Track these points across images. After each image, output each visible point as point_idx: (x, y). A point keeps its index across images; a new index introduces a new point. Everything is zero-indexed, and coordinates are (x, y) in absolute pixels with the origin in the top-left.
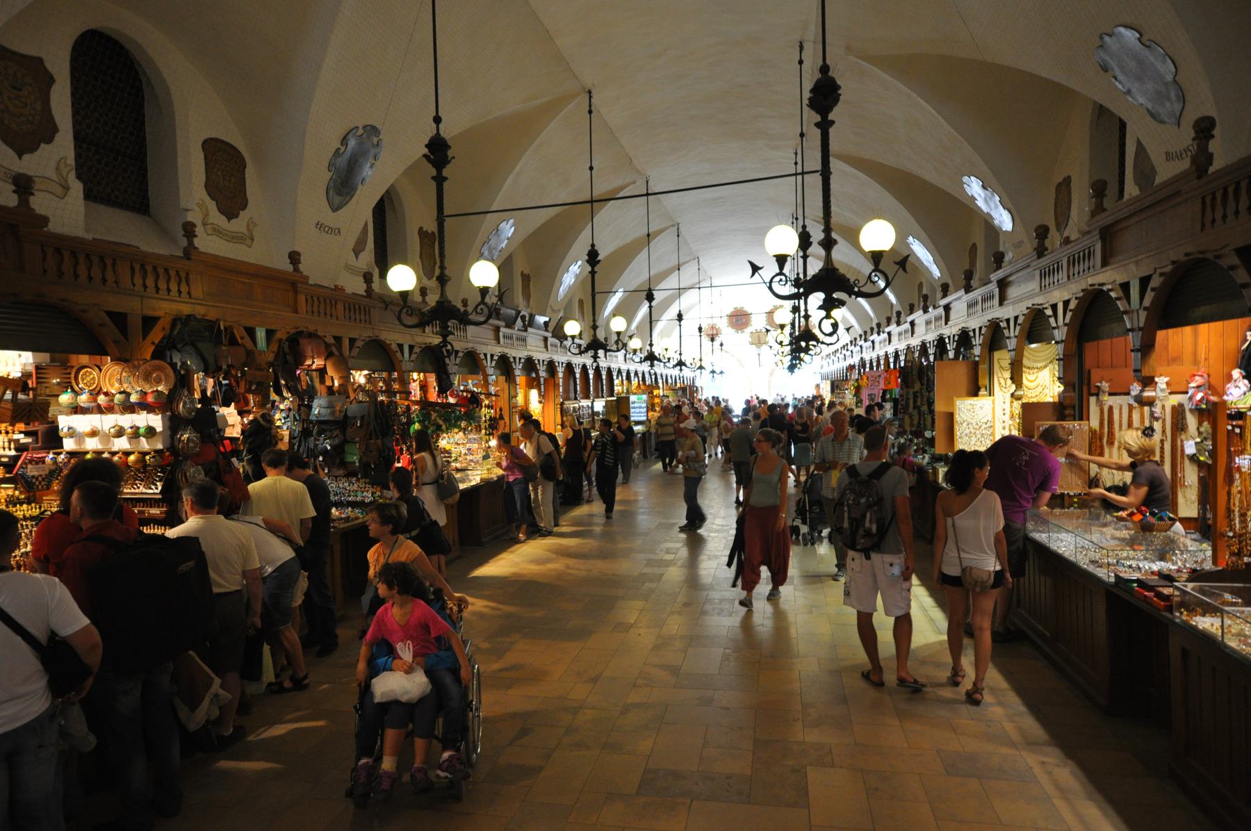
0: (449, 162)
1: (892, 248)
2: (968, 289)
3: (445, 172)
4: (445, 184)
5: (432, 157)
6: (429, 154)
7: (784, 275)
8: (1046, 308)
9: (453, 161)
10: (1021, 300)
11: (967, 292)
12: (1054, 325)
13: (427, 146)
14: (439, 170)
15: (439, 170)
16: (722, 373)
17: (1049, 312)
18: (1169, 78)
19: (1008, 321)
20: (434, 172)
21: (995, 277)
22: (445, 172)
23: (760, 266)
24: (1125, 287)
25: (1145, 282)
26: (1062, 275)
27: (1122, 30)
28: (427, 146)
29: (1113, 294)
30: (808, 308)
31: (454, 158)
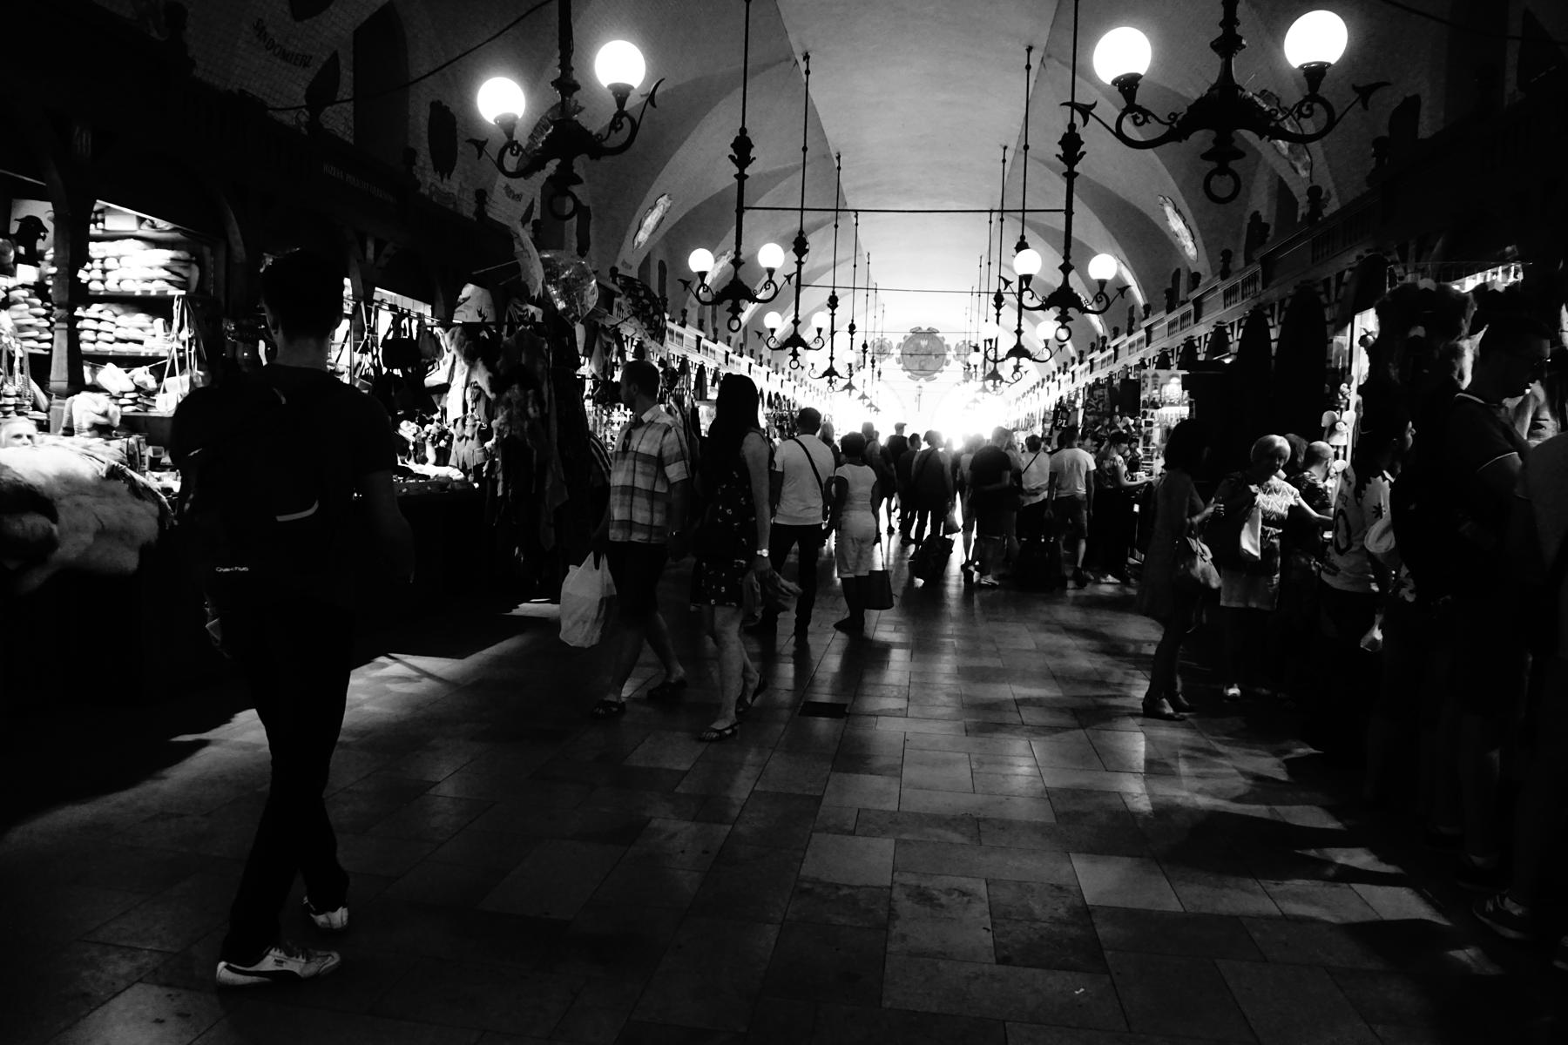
0: (751, 162)
4: (745, 181)
5: (736, 157)
6: (733, 154)
7: (1030, 290)
9: (754, 162)
13: (732, 146)
14: (742, 169)
15: (742, 169)
17: (1228, 330)
20: (736, 171)
22: (747, 171)
23: (1011, 280)
31: (754, 158)
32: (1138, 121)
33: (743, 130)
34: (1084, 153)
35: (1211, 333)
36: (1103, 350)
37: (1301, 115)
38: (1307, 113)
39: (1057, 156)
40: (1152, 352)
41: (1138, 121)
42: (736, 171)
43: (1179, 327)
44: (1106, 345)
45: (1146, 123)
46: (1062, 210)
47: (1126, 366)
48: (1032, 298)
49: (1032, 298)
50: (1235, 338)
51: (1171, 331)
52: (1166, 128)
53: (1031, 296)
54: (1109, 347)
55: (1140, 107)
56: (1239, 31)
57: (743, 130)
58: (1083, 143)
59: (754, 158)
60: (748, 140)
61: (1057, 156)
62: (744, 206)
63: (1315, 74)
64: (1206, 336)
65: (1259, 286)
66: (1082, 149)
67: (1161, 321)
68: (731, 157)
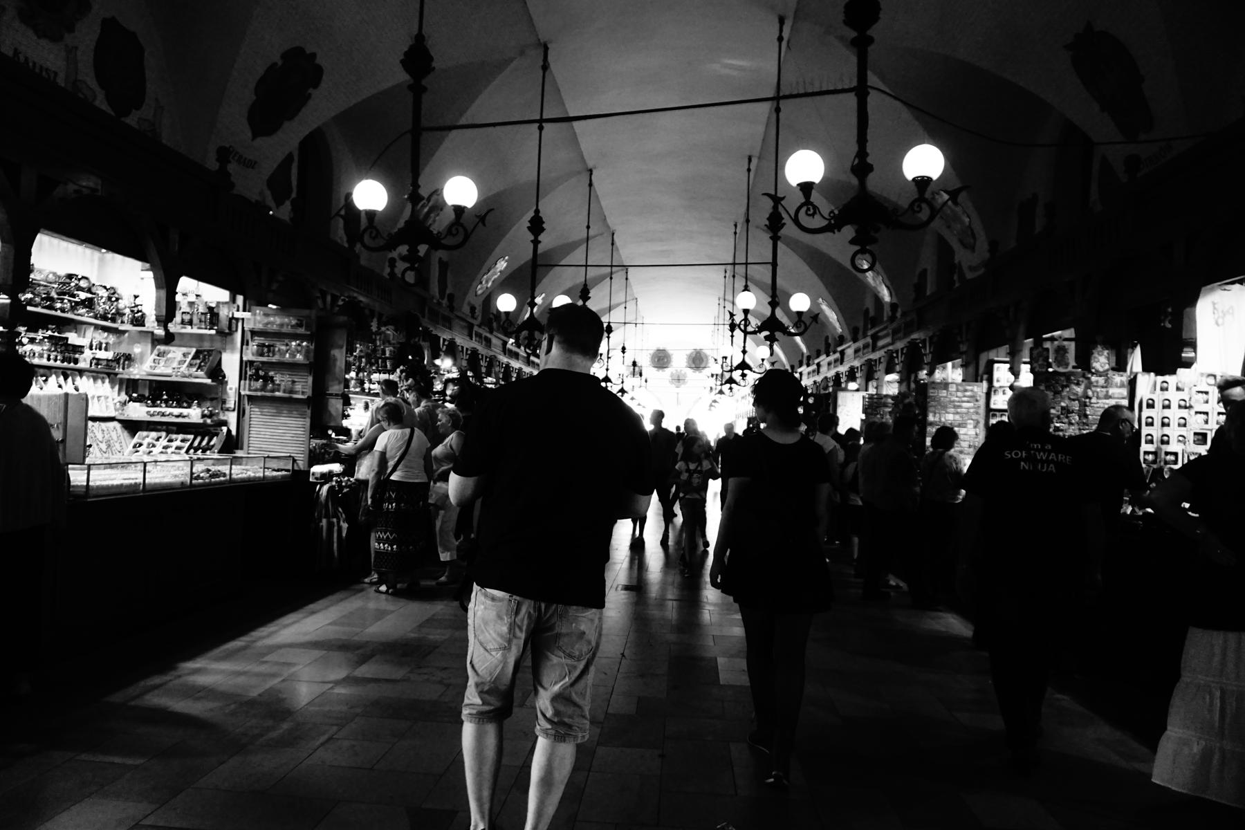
1: (809, 309)
2: (855, 340)
8: (893, 353)
10: (883, 347)
11: (854, 342)
12: (897, 362)
16: (644, 407)
17: (895, 355)
18: (967, 224)
19: (876, 360)
20: (532, 238)
21: (870, 333)
22: (540, 238)
24: (924, 341)
25: (931, 338)
26: (901, 335)
27: (942, 192)
28: (529, 221)
29: (921, 345)
30: (746, 345)
32: (809, 213)
33: (537, 211)
36: (808, 365)
37: (915, 212)
38: (918, 209)
40: (843, 369)
41: (809, 213)
42: (532, 238)
43: (861, 353)
44: (811, 362)
45: (811, 217)
47: (826, 378)
50: (900, 361)
51: (856, 355)
52: (825, 223)
54: (814, 364)
55: (812, 203)
56: (869, 160)
57: (537, 211)
60: (541, 218)
63: (922, 183)
66: (783, 221)
67: (849, 347)
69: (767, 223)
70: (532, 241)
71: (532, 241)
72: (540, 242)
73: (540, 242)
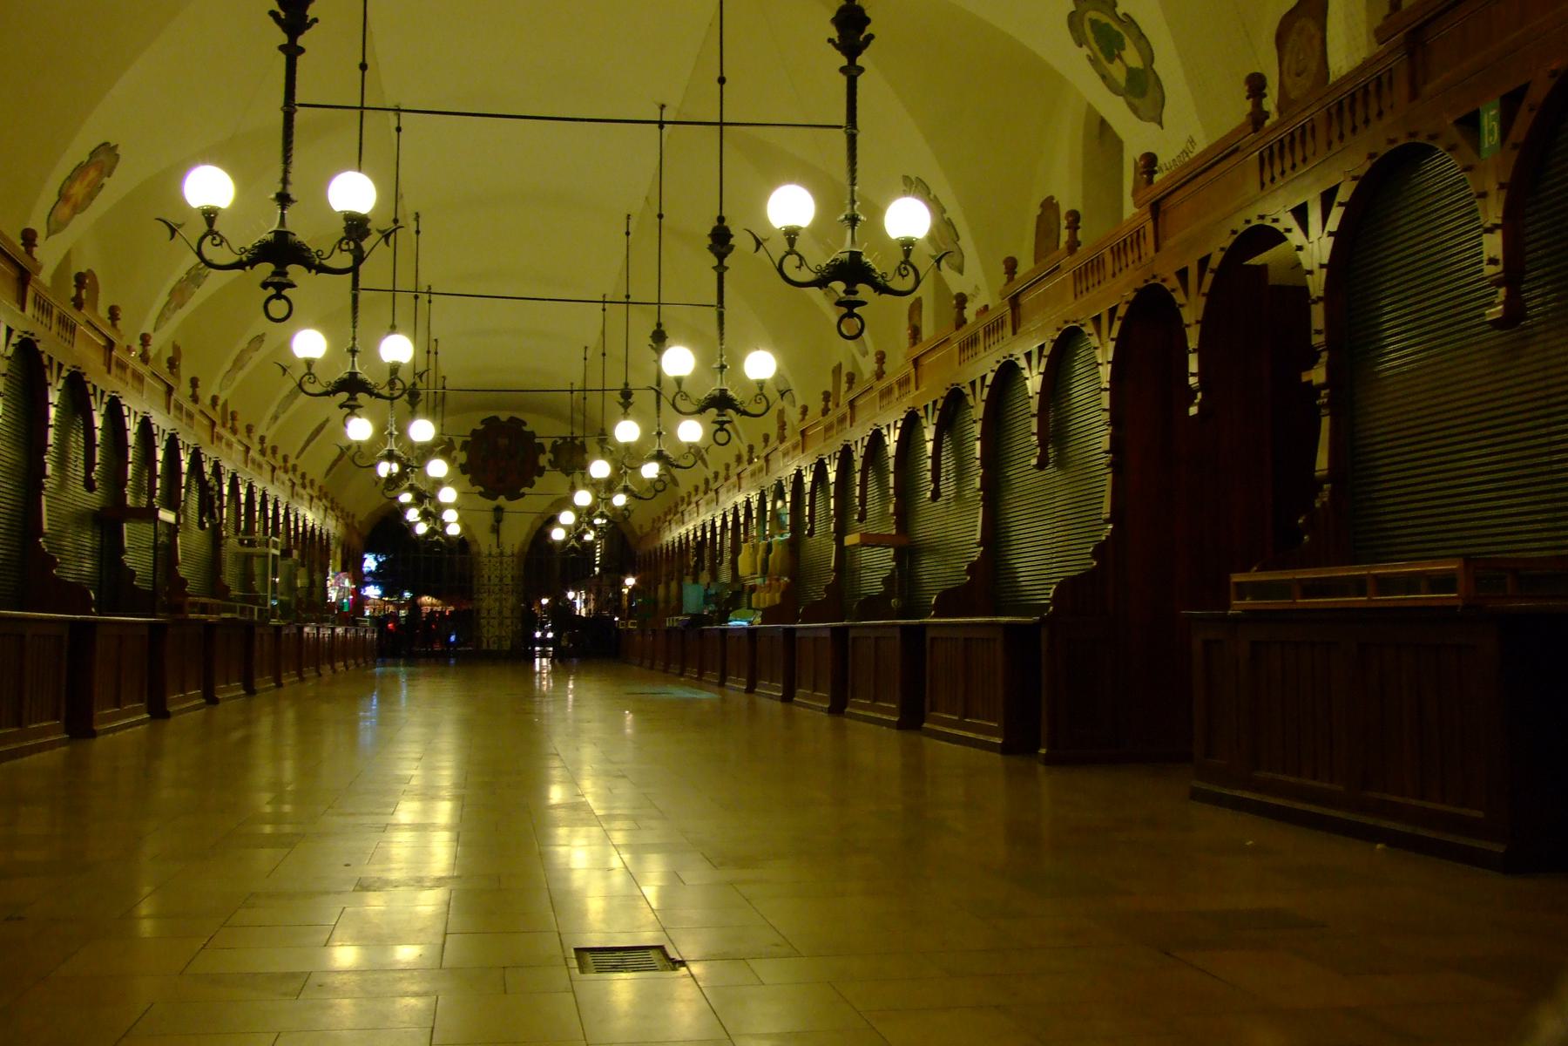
0: (309, 26)
3: (301, 41)
5: (283, 15)
17: (1089, 329)
20: (283, 39)
22: (301, 41)
31: (316, 20)
34: (870, 37)
35: (1052, 341)
39: (830, 40)
46: (840, 127)
48: (797, 267)
49: (799, 267)
53: (798, 263)
58: (868, 21)
59: (316, 20)
61: (830, 40)
62: (296, 103)
64: (1041, 348)
65: (1148, 246)
66: (869, 30)
68: (273, 14)
69: (834, 34)
70: (282, 48)
71: (282, 48)
72: (302, 51)
73: (302, 51)
